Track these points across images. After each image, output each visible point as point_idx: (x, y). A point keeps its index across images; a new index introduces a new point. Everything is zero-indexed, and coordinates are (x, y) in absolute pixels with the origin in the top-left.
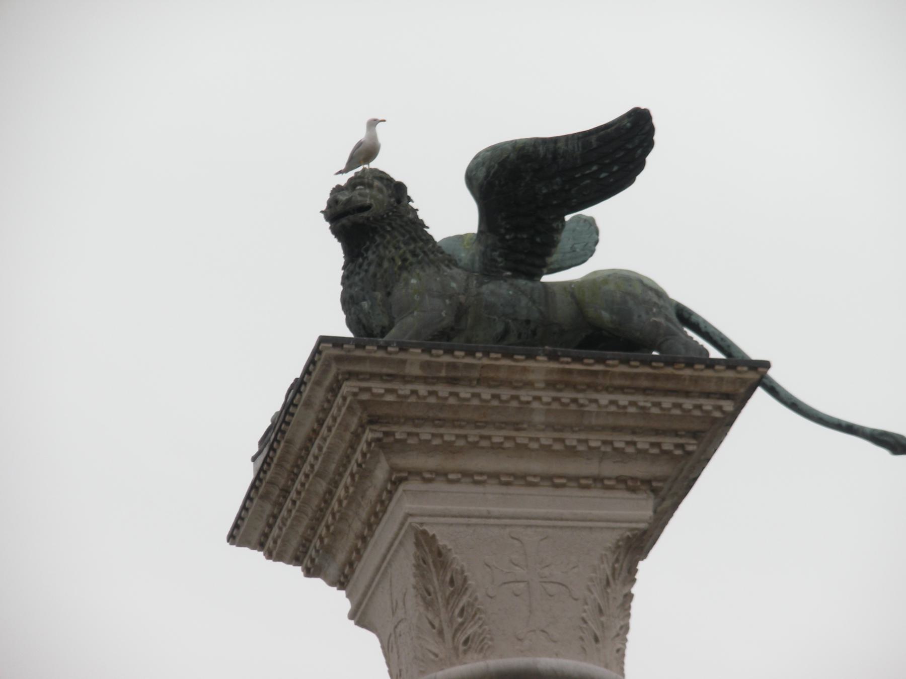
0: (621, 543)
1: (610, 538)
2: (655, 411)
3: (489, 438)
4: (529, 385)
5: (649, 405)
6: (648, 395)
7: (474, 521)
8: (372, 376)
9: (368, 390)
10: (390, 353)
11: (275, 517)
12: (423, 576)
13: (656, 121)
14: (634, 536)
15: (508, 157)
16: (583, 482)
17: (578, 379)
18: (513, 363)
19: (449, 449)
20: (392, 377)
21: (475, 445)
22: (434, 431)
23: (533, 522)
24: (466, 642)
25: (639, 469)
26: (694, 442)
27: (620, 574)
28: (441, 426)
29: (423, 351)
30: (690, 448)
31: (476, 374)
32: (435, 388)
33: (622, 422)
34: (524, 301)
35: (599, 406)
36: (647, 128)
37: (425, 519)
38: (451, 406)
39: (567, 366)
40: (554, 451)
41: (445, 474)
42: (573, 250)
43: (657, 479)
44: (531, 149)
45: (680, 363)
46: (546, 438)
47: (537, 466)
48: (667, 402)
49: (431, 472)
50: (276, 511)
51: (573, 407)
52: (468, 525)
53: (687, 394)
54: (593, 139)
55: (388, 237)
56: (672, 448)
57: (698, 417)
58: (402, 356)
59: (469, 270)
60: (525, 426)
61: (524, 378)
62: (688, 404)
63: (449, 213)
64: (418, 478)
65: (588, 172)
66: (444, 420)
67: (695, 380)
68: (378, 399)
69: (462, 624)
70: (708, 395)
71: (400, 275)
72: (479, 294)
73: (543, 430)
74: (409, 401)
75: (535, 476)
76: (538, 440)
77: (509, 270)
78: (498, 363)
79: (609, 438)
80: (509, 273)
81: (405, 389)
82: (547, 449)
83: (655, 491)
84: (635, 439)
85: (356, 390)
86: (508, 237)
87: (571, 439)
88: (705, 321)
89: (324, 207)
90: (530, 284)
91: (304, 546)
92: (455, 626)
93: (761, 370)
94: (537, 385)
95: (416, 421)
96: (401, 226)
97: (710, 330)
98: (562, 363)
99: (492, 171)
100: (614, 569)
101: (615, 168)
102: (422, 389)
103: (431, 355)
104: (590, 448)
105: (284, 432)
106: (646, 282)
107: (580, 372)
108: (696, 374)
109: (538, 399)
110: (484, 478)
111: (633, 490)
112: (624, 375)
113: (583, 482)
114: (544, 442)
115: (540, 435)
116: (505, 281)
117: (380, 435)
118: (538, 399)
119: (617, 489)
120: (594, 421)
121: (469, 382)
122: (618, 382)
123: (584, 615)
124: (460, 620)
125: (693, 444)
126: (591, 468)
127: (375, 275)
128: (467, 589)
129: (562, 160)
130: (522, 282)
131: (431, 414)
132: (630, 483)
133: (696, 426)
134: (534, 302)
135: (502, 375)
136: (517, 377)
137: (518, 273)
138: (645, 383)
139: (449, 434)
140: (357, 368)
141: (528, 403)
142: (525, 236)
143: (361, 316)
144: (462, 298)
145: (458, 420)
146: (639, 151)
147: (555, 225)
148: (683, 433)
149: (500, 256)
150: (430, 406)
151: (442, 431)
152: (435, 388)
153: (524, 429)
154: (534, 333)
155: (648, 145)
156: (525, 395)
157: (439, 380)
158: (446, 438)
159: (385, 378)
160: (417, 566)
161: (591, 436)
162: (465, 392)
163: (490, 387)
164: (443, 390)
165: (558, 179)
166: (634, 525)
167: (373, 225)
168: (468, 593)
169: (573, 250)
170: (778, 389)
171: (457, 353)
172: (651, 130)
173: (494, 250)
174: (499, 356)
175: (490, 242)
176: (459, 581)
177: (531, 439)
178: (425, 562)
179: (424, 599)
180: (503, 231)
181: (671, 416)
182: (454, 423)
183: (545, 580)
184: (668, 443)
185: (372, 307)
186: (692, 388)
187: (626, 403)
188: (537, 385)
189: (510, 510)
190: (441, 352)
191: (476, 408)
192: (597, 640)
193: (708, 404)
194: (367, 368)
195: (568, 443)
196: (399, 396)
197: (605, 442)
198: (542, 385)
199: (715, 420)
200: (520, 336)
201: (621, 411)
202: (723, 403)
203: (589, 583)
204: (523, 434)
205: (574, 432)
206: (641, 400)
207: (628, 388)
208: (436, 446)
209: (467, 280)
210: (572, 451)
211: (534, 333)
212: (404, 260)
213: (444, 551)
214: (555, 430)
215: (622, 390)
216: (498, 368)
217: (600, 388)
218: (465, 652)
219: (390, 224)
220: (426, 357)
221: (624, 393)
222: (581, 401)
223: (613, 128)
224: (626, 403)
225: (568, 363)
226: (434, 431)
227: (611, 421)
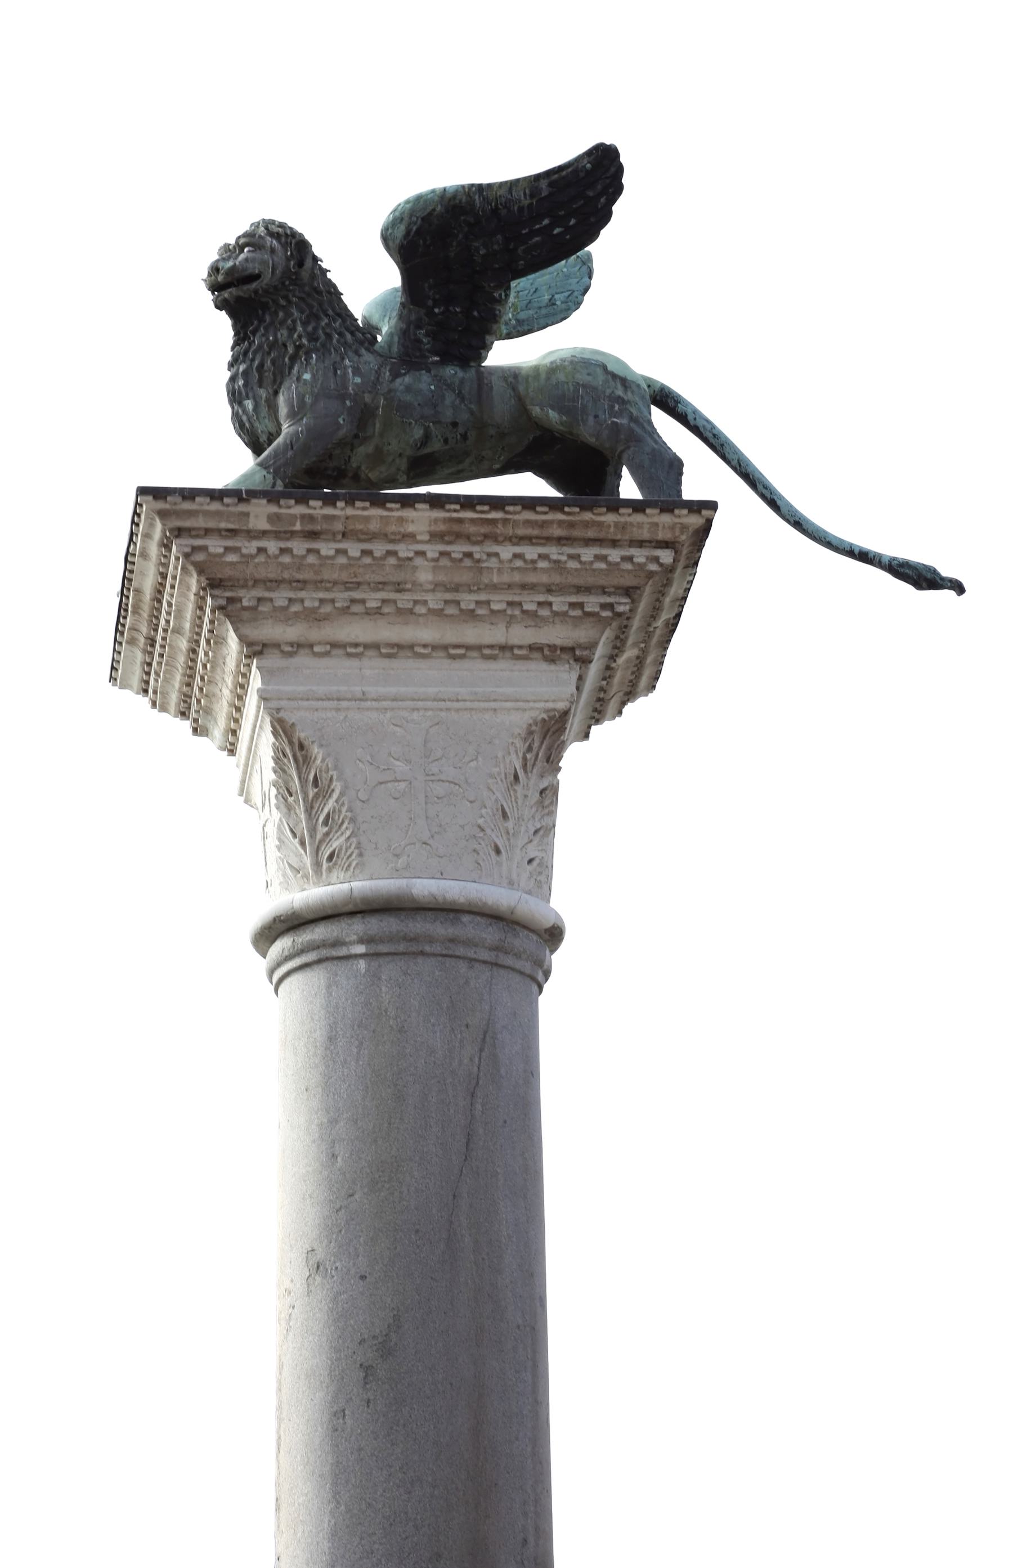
0: (534, 728)
1: (520, 720)
2: (573, 565)
3: (363, 601)
5: (564, 558)
6: (564, 545)
7: (344, 704)
8: (207, 532)
9: (204, 548)
10: (228, 505)
11: (150, 665)
12: (284, 771)
14: (551, 718)
15: (434, 210)
16: (487, 651)
17: (472, 529)
18: (385, 513)
19: (312, 616)
20: (233, 533)
21: (345, 611)
22: (292, 595)
23: (420, 704)
24: (330, 858)
25: (557, 635)
26: (627, 600)
27: (534, 765)
28: (302, 589)
29: (269, 501)
30: (621, 609)
31: (339, 527)
32: (289, 544)
33: (531, 578)
34: (450, 398)
35: (501, 561)
36: (613, 170)
37: (283, 703)
38: (311, 565)
39: (455, 515)
40: (446, 616)
41: (311, 646)
42: (552, 303)
43: (580, 646)
44: (464, 200)
45: (600, 506)
46: (434, 600)
47: (425, 633)
48: (588, 554)
49: (292, 645)
50: (148, 660)
51: (468, 562)
52: (338, 710)
53: (614, 543)
54: (544, 184)
55: (281, 314)
56: (597, 609)
57: (629, 571)
58: (242, 508)
59: (384, 356)
60: (409, 586)
61: (402, 530)
62: (614, 555)
63: (366, 280)
64: (276, 651)
65: (537, 227)
66: (305, 582)
67: (623, 527)
68: (218, 559)
69: (327, 834)
70: (641, 544)
71: (291, 368)
72: (390, 391)
73: (433, 590)
74: (256, 560)
75: (425, 646)
76: (425, 602)
77: (437, 355)
78: (366, 513)
79: (517, 599)
80: (437, 359)
81: (250, 547)
82: (439, 613)
83: (577, 660)
84: (551, 599)
85: (188, 550)
86: (436, 310)
87: (467, 601)
88: (695, 411)
89: (205, 275)
90: (461, 374)
91: (185, 702)
92: (319, 836)
93: (704, 512)
94: (419, 538)
95: (268, 584)
96: (301, 299)
97: (700, 423)
98: (449, 511)
99: (414, 228)
100: (525, 759)
101: (573, 222)
102: (272, 546)
103: (280, 507)
104: (492, 611)
105: (130, 580)
106: (610, 367)
107: (472, 521)
108: (622, 519)
109: (422, 554)
110: (360, 649)
111: (552, 660)
112: (528, 523)
113: (487, 651)
114: (432, 605)
115: (429, 597)
116: (429, 371)
117: (223, 602)
118: (422, 554)
119: (531, 659)
120: (495, 580)
121: (333, 537)
122: (521, 532)
123: (481, 821)
124: (326, 829)
125: (625, 604)
126: (495, 634)
127: (261, 365)
128: (333, 790)
129: (505, 211)
130: (450, 371)
131: (286, 575)
132: (546, 652)
133: (628, 581)
134: (463, 399)
135: (374, 526)
136: (393, 528)
137: (447, 358)
138: (557, 532)
139: (311, 598)
140: (187, 524)
141: (410, 559)
142: (458, 310)
143: (244, 418)
144: (368, 398)
145: (321, 582)
146: (603, 200)
147: (496, 295)
148: (612, 590)
149: (427, 335)
150: (285, 567)
151: (302, 594)
152: (289, 544)
153: (408, 590)
154: (465, 437)
155: (615, 189)
156: (404, 550)
157: (293, 534)
158: (308, 604)
159: (223, 533)
160: (277, 760)
161: (492, 597)
162: (327, 549)
163: (360, 540)
164: (299, 546)
165: (499, 237)
166: (550, 705)
167: (264, 300)
168: (335, 796)
169: (552, 303)
170: (779, 502)
171: (312, 503)
172: (620, 169)
173: (419, 327)
174: (367, 504)
175: (413, 317)
176: (323, 782)
177: (416, 602)
178: (284, 755)
179: (286, 800)
180: (430, 303)
181: (594, 570)
182: (318, 584)
183: (433, 778)
184: (592, 602)
185: (255, 409)
186: (619, 537)
187: (535, 557)
188: (419, 538)
189: (393, 690)
190: (293, 502)
191: (343, 567)
192: (498, 851)
193: (640, 555)
194: (200, 522)
195: (463, 606)
196: (243, 556)
197: (510, 604)
198: (427, 537)
199: (651, 574)
200: (446, 441)
201: (530, 566)
203: (490, 781)
204: (407, 596)
205: (471, 591)
206: (553, 552)
207: (537, 537)
208: (296, 613)
209: (378, 373)
210: (470, 615)
211: (465, 437)
212: (298, 347)
213: (306, 743)
214: (447, 590)
215: (529, 540)
216: (367, 519)
217: (501, 539)
218: (329, 870)
219: (286, 298)
220: (273, 509)
221: (533, 544)
222: (477, 556)
223: (570, 170)
224: (535, 557)
225: (455, 511)
226: (292, 595)
227: (517, 578)
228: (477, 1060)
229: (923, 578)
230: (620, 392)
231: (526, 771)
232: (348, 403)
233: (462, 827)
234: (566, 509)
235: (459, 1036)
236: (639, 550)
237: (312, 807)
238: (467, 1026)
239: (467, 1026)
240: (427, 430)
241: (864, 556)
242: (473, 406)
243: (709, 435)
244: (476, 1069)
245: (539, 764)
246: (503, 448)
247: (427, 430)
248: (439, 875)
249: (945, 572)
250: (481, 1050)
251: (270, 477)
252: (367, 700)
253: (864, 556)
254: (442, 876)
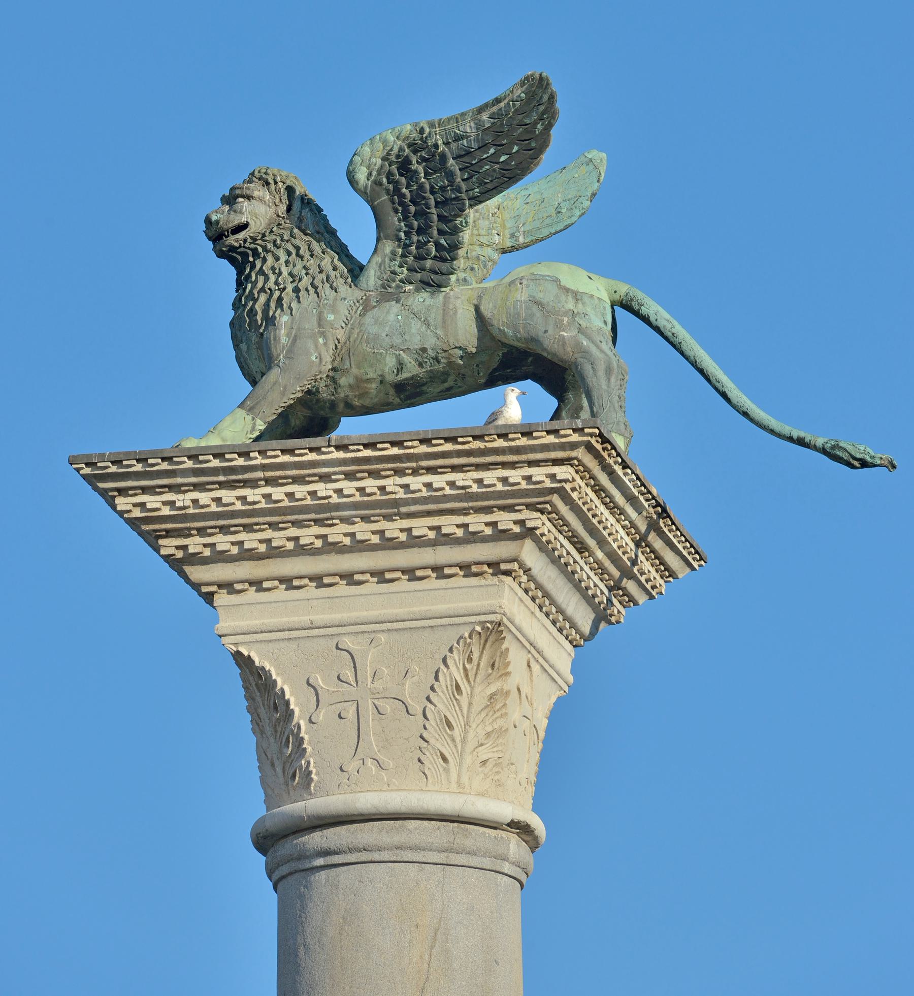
13: (555, 87)
34: (416, 326)
39: (360, 454)
101: (515, 149)
130: (422, 299)
134: (428, 325)
143: (242, 359)
155: (549, 115)
176: (281, 708)
183: (377, 696)
185: (248, 350)
189: (337, 617)
192: (445, 759)
202: (556, 470)
228: (427, 956)
230: (570, 305)
231: (469, 681)
232: (321, 340)
233: (407, 739)
234: (460, 440)
235: (408, 937)
236: (537, 469)
237: (276, 732)
238: (417, 926)
239: (417, 926)
240: (398, 357)
241: (801, 442)
242: (438, 331)
243: (669, 334)
244: (426, 965)
245: (482, 672)
246: (477, 366)
247: (398, 357)
248: (386, 787)
250: (432, 947)
251: (249, 418)
252: (313, 628)
253: (801, 442)
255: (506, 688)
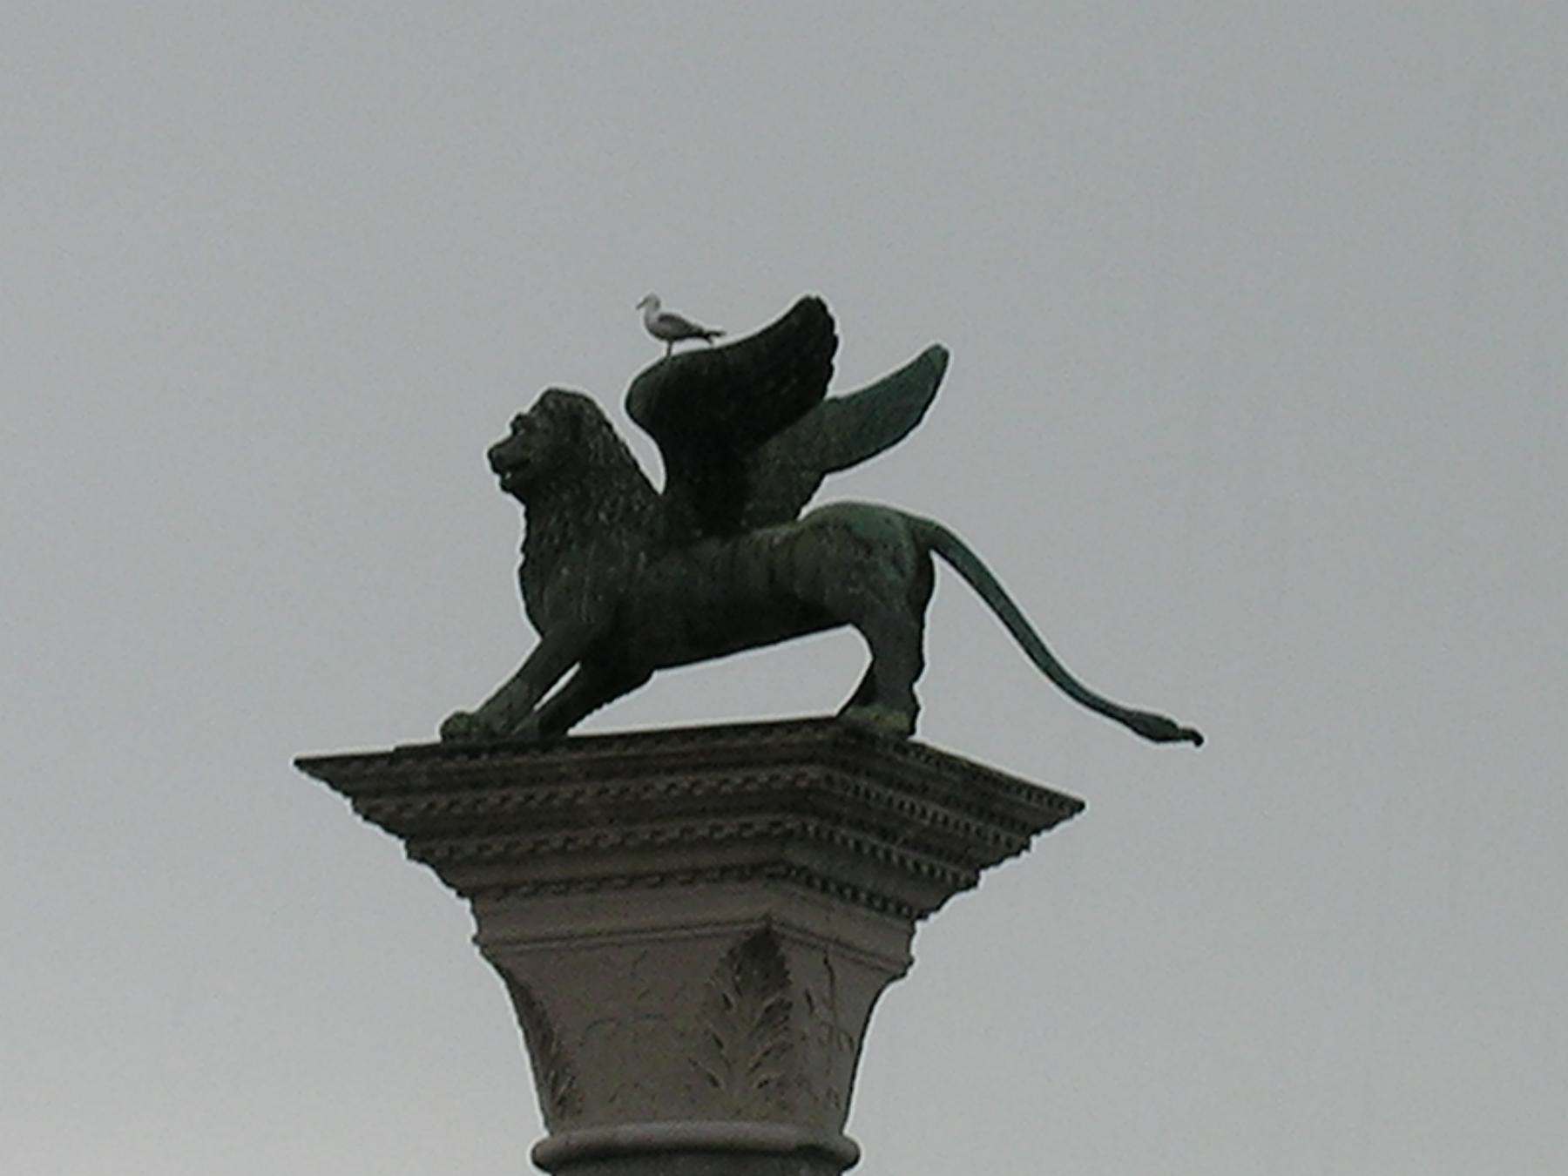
4: (561, 778)
13: (831, 310)
75: (623, 877)
110: (562, 887)
111: (742, 878)
130: (712, 549)
162: (493, 798)
164: (467, 797)
192: (715, 1083)
210: (648, 848)
229: (1157, 729)
249: (1182, 724)
254: (655, 1117)
255: (788, 999)
